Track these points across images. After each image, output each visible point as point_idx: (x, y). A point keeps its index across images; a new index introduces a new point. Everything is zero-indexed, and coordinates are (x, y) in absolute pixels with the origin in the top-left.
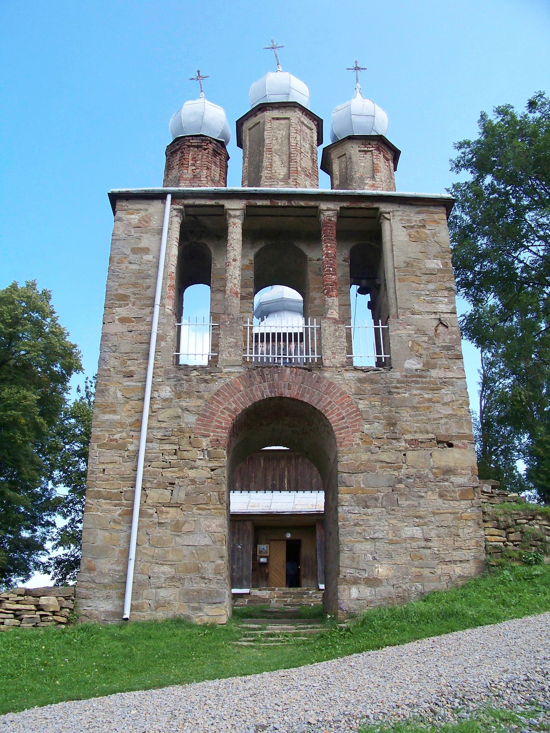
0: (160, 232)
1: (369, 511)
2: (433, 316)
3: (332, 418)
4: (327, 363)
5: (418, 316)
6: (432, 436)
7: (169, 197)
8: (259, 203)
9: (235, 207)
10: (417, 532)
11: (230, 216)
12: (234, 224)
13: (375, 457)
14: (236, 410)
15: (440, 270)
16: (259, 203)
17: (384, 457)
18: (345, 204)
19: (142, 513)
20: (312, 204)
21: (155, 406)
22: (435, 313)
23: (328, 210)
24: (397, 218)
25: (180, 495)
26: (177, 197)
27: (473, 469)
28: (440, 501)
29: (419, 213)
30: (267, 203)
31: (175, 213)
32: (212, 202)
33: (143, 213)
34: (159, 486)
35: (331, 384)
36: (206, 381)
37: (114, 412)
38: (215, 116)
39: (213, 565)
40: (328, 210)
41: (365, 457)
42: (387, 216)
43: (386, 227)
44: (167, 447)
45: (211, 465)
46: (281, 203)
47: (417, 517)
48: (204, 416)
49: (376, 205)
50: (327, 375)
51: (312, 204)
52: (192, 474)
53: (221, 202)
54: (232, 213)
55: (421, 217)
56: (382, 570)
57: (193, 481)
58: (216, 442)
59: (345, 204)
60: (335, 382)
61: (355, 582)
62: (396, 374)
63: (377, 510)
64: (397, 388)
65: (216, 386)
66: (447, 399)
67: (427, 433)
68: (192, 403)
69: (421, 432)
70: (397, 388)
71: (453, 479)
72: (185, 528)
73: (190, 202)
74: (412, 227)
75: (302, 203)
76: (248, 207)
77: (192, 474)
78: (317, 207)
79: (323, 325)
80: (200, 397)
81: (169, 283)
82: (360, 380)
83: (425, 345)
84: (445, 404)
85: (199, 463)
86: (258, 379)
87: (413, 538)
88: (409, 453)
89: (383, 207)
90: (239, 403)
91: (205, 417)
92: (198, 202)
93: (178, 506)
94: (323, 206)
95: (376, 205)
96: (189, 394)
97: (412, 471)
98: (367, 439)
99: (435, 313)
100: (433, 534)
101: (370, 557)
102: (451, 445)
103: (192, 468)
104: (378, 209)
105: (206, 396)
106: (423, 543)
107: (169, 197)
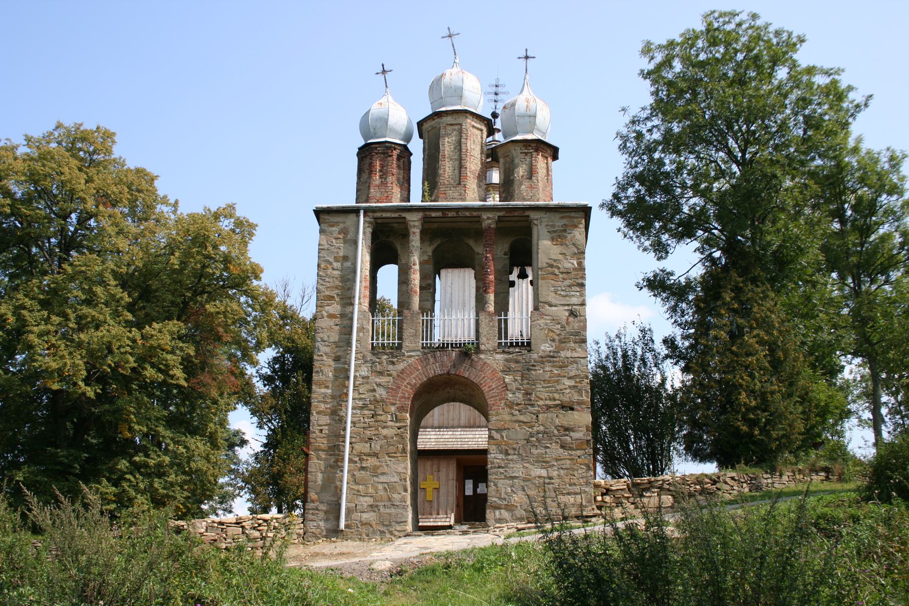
0: (355, 243)
1: (510, 457)
2: (566, 308)
3: (485, 389)
4: (482, 347)
5: (554, 308)
6: (559, 402)
7: (362, 212)
8: (433, 214)
10: (543, 473)
12: (414, 233)
13: (514, 418)
14: (415, 384)
15: (575, 269)
16: (433, 214)
17: (522, 418)
18: (501, 214)
19: (350, 461)
20: (475, 214)
21: (357, 383)
22: (568, 305)
23: (488, 218)
24: (544, 224)
25: (376, 446)
26: (367, 211)
27: (587, 426)
28: (562, 450)
29: (562, 218)
30: (439, 214)
31: (367, 225)
32: (396, 215)
33: (342, 226)
34: (362, 440)
35: (485, 363)
36: (393, 363)
38: (401, 116)
39: (400, 496)
40: (488, 218)
42: (535, 222)
44: (366, 412)
45: (398, 425)
47: (544, 462)
48: (392, 389)
52: (385, 432)
53: (404, 215)
54: (412, 223)
55: (564, 221)
57: (385, 437)
58: (402, 409)
60: (488, 361)
61: (498, 508)
62: (535, 356)
63: (515, 457)
64: (534, 366)
65: (401, 366)
66: (572, 374)
67: (555, 400)
68: (383, 380)
69: (550, 399)
70: (534, 366)
71: (572, 434)
72: (379, 471)
73: (378, 215)
74: (555, 232)
75: (467, 214)
77: (385, 432)
79: (481, 317)
80: (389, 375)
81: (364, 284)
82: (507, 360)
83: (558, 332)
84: (570, 378)
85: (390, 423)
86: (432, 360)
87: (540, 477)
88: (540, 416)
89: (533, 215)
90: (417, 379)
92: (385, 215)
93: (376, 455)
96: (381, 373)
97: (542, 428)
98: (510, 405)
99: (568, 305)
100: (555, 473)
101: (509, 490)
102: (572, 409)
103: (384, 427)
104: (528, 216)
105: (395, 374)
106: (547, 481)
107: (362, 212)
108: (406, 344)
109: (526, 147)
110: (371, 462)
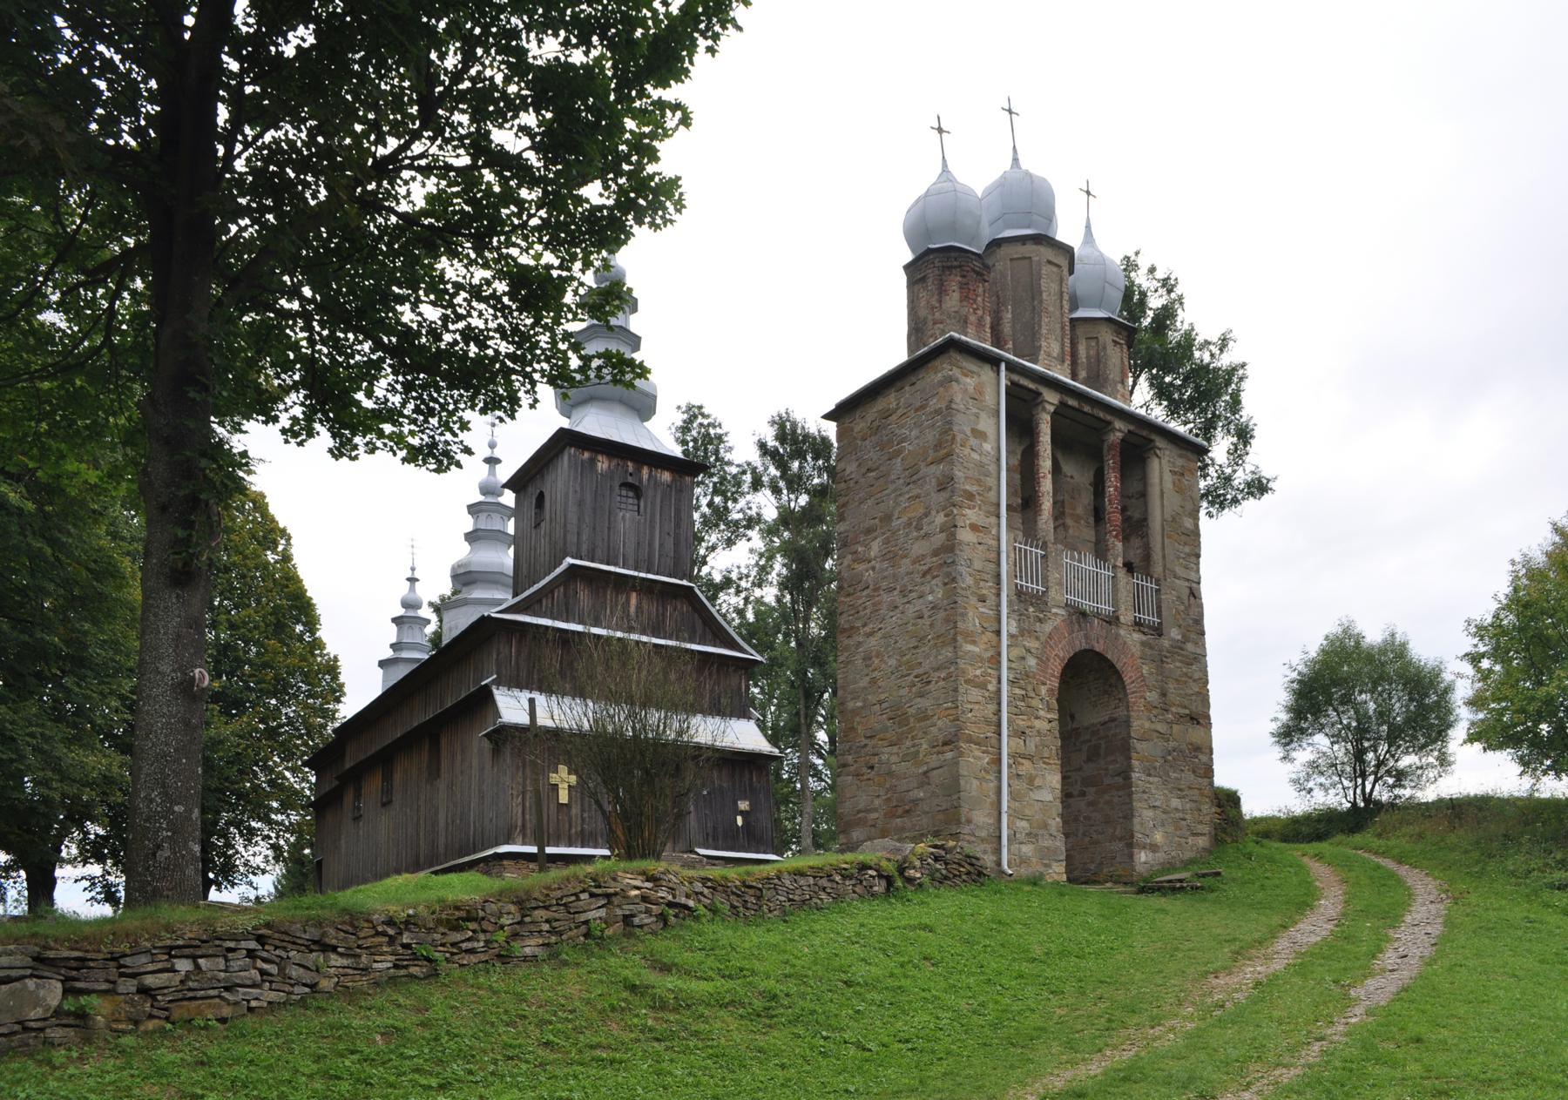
7: (1003, 366)
10: (1175, 803)
11: (1044, 409)
18: (1132, 428)
20: (1109, 418)
26: (1012, 368)
29: (1180, 456)
32: (1032, 386)
36: (1040, 620)
37: (974, 643)
41: (1147, 725)
46: (1087, 409)
49: (1153, 437)
50: (1122, 632)
51: (1109, 418)
53: (1042, 389)
56: (1158, 837)
59: (1132, 428)
68: (1033, 644)
72: (1037, 782)
75: (1101, 415)
76: (1062, 404)
77: (1037, 724)
80: (1037, 638)
89: (1160, 442)
91: (1043, 661)
93: (1030, 758)
94: (1118, 424)
95: (1153, 437)
108: (1052, 593)
109: (1118, 334)
110: (1026, 767)
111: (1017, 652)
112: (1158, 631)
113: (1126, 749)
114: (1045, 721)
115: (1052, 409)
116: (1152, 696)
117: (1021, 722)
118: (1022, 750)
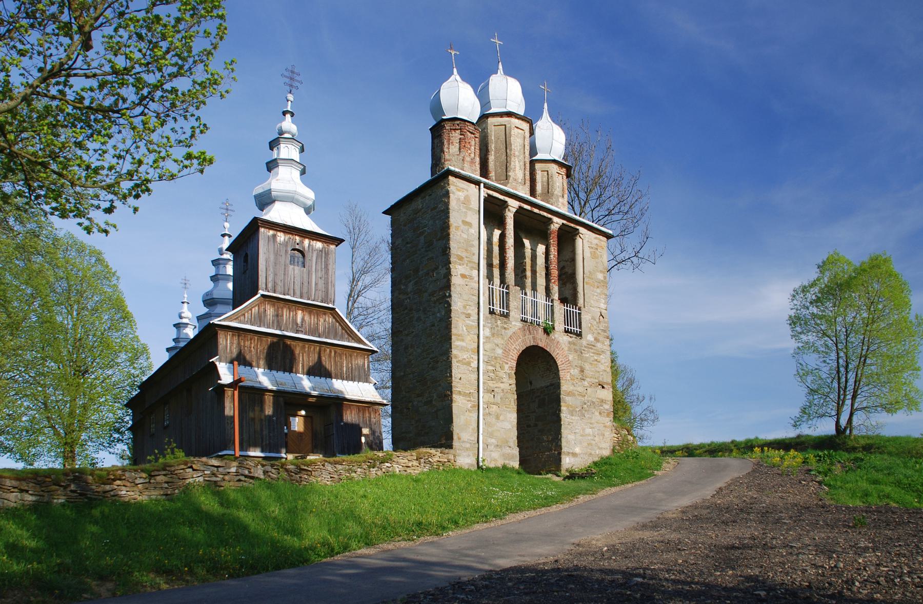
3: (559, 362)
9: (514, 204)
20: (550, 216)
37: (463, 340)
43: (579, 242)
46: (536, 211)
51: (550, 216)
53: (507, 199)
59: (565, 222)
68: (499, 341)
76: (520, 207)
77: (502, 386)
78: (550, 219)
80: (503, 339)
89: (582, 230)
91: (506, 351)
94: (555, 219)
108: (512, 314)
111: (488, 346)
112: (579, 335)
113: (557, 401)
114: (508, 384)
115: (514, 210)
116: (575, 372)
117: (492, 384)
118: (492, 400)
